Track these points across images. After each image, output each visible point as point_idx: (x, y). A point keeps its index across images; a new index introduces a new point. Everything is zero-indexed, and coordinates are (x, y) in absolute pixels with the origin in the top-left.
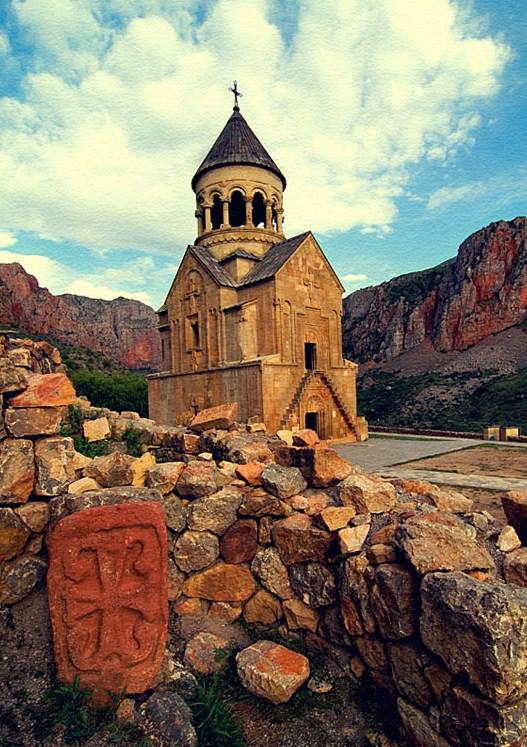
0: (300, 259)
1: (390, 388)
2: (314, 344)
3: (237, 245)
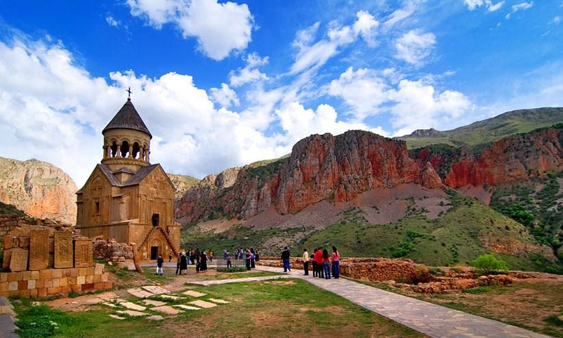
1: (247, 238)
2: (158, 215)
3: (123, 166)
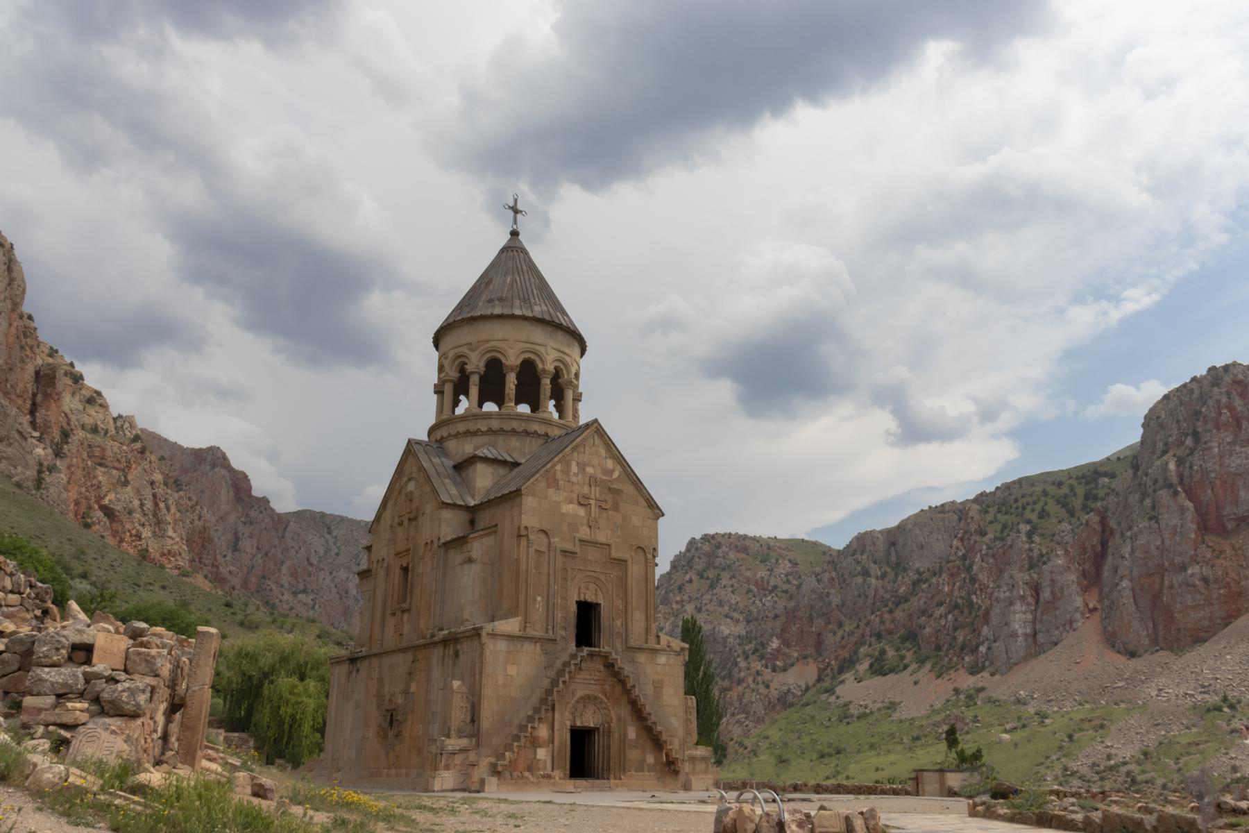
0: (574, 463)
2: (598, 605)
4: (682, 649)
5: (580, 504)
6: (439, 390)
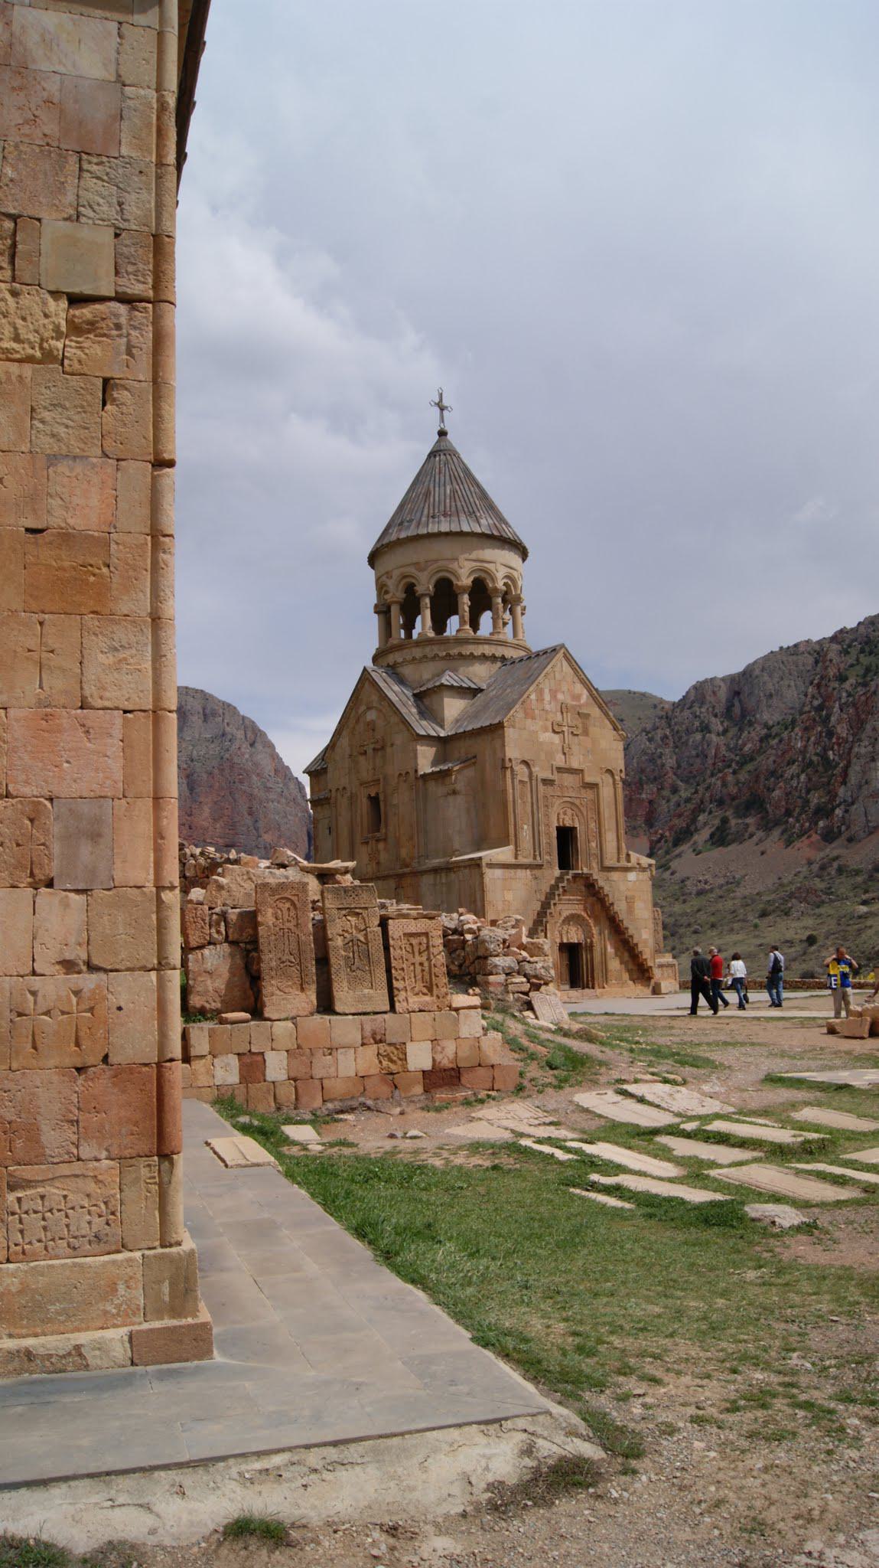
0: (547, 691)
2: (573, 829)
4: (650, 865)
5: (554, 732)
6: (383, 610)
